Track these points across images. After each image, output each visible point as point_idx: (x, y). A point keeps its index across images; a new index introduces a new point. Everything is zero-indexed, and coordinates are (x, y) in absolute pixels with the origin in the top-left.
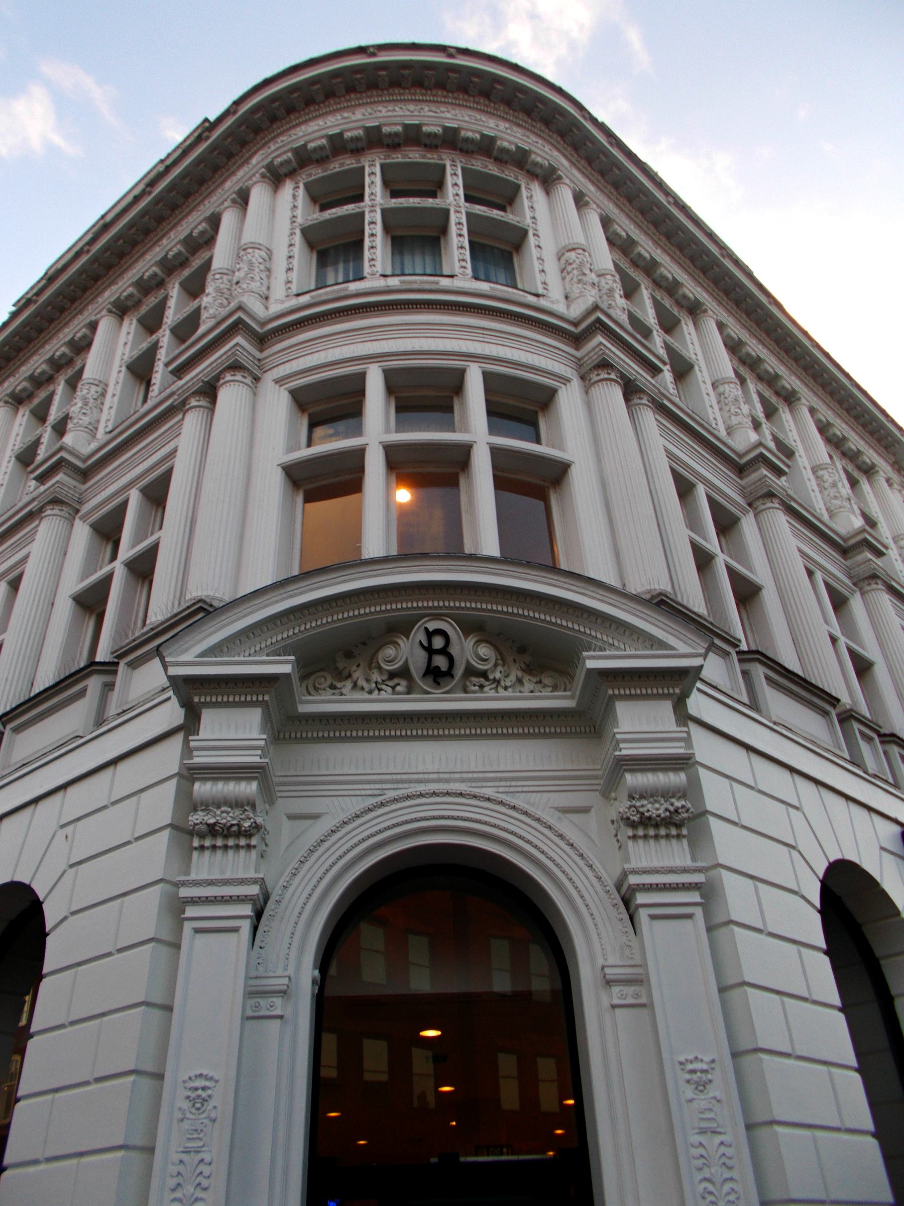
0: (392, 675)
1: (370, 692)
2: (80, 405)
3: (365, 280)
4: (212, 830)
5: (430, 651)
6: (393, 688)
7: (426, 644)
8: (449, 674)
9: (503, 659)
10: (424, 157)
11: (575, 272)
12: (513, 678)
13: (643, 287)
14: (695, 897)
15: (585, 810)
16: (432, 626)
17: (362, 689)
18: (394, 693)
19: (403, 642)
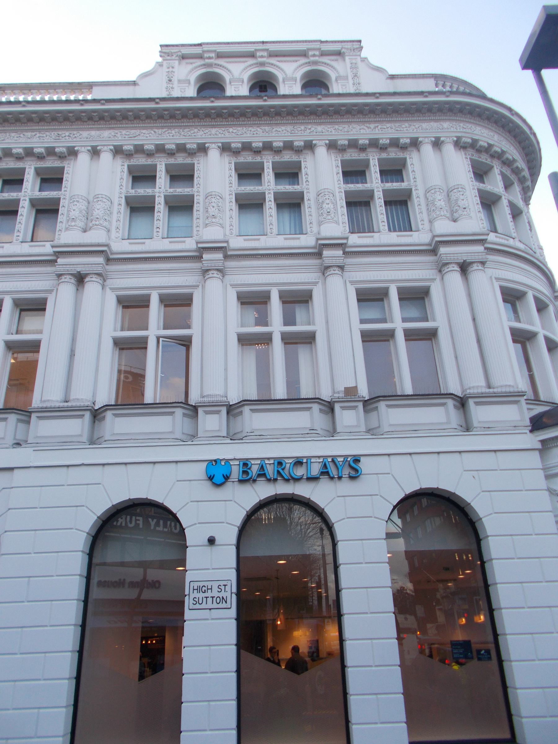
2: (331, 206)
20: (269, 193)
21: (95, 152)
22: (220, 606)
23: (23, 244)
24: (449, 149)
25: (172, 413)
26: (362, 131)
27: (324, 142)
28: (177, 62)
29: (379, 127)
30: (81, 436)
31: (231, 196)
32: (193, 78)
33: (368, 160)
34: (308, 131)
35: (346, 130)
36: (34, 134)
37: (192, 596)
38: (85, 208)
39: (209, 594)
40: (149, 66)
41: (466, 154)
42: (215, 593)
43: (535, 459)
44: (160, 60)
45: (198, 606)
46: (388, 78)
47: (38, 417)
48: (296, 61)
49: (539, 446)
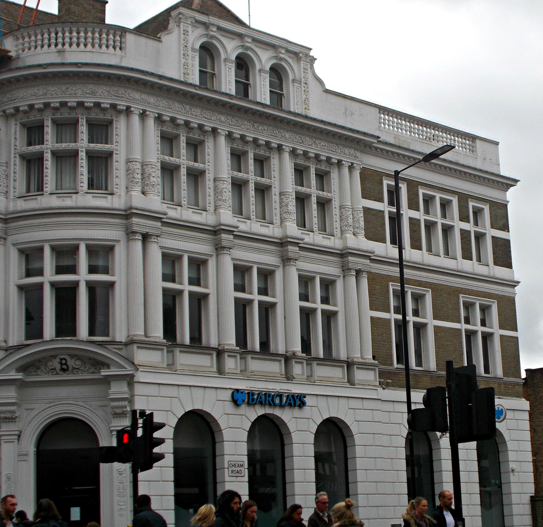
0: (52, 369)
1: (46, 373)
3: (44, 196)
5: (62, 364)
6: (52, 372)
7: (60, 362)
8: (67, 370)
9: (85, 363)
11: (131, 175)
12: (87, 368)
13: (181, 135)
15: (106, 406)
16: (62, 357)
17: (44, 372)
18: (52, 375)
19: (54, 360)
41: (16, 120)
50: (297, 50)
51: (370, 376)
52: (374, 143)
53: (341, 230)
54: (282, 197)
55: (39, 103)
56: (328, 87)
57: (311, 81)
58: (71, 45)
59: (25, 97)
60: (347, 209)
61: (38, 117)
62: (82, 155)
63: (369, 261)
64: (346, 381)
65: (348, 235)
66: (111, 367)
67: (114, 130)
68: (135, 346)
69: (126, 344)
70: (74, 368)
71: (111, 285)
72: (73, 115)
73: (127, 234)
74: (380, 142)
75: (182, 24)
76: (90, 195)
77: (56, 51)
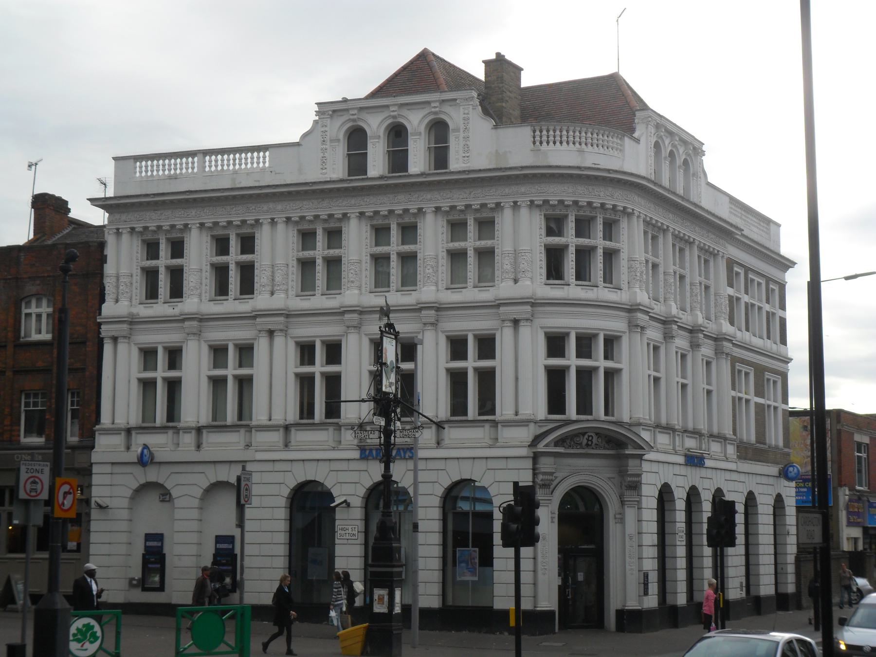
2: (431, 271)
4: (543, 485)
5: (588, 440)
8: (591, 445)
10: (591, 213)
14: (636, 503)
15: (614, 478)
16: (590, 434)
19: (581, 436)
20: (393, 254)
21: (273, 222)
22: (353, 538)
23: (236, 301)
24: (524, 212)
25: (327, 429)
26: (461, 197)
27: (431, 209)
28: (329, 120)
29: (474, 192)
30: (278, 442)
31: (367, 258)
32: (341, 136)
33: (466, 219)
34: (421, 199)
35: (448, 197)
36: (232, 207)
37: (339, 532)
38: (270, 273)
39: (347, 532)
40: (308, 127)
41: (541, 211)
42: (350, 532)
43: (529, 464)
44: (317, 118)
45: (342, 537)
46: (492, 128)
47: (256, 430)
48: (423, 108)
49: (532, 455)
50: (697, 145)
51: (731, 450)
52: (738, 234)
53: (715, 316)
54: (693, 287)
55: (569, 200)
56: (711, 180)
57: (702, 176)
58: (586, 144)
59: (555, 192)
60: (721, 297)
61: (563, 212)
62: (600, 252)
63: (731, 345)
64: (723, 455)
65: (723, 321)
66: (629, 447)
67: (621, 230)
68: (642, 427)
69: (630, 425)
70: (596, 444)
71: (618, 371)
72: (593, 214)
73: (629, 326)
74: (743, 235)
75: (649, 126)
76: (606, 290)
77: (575, 149)
